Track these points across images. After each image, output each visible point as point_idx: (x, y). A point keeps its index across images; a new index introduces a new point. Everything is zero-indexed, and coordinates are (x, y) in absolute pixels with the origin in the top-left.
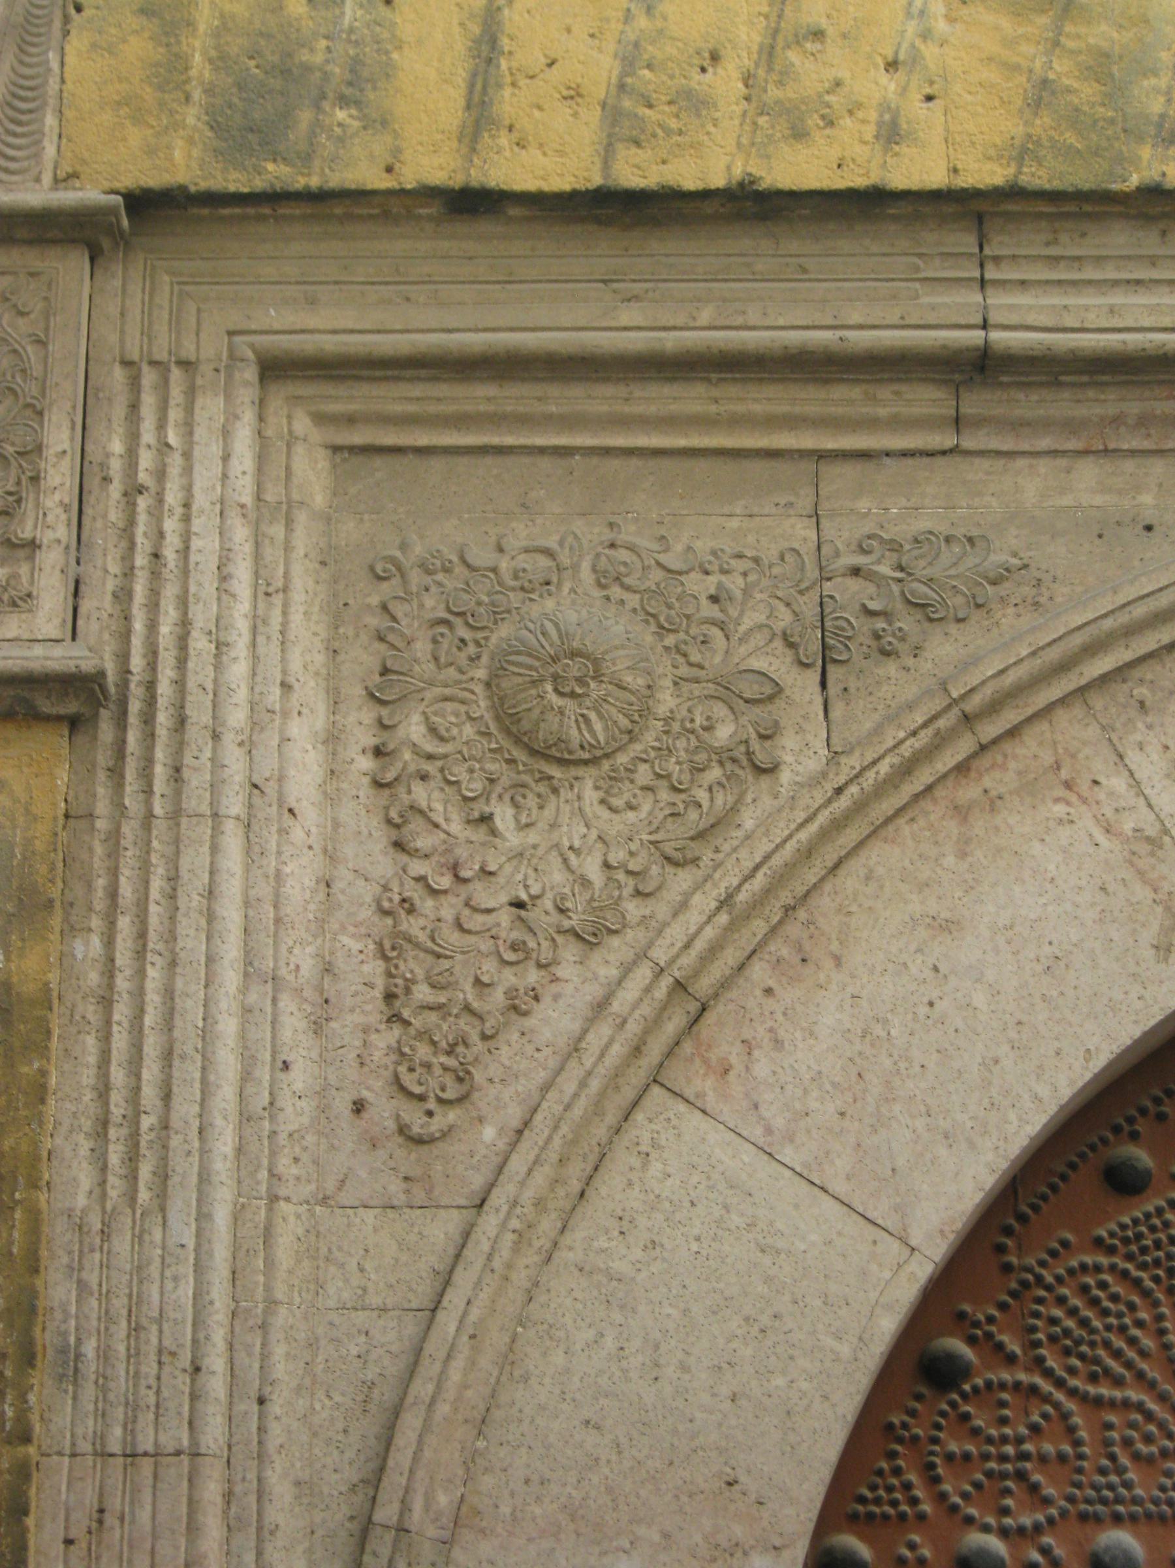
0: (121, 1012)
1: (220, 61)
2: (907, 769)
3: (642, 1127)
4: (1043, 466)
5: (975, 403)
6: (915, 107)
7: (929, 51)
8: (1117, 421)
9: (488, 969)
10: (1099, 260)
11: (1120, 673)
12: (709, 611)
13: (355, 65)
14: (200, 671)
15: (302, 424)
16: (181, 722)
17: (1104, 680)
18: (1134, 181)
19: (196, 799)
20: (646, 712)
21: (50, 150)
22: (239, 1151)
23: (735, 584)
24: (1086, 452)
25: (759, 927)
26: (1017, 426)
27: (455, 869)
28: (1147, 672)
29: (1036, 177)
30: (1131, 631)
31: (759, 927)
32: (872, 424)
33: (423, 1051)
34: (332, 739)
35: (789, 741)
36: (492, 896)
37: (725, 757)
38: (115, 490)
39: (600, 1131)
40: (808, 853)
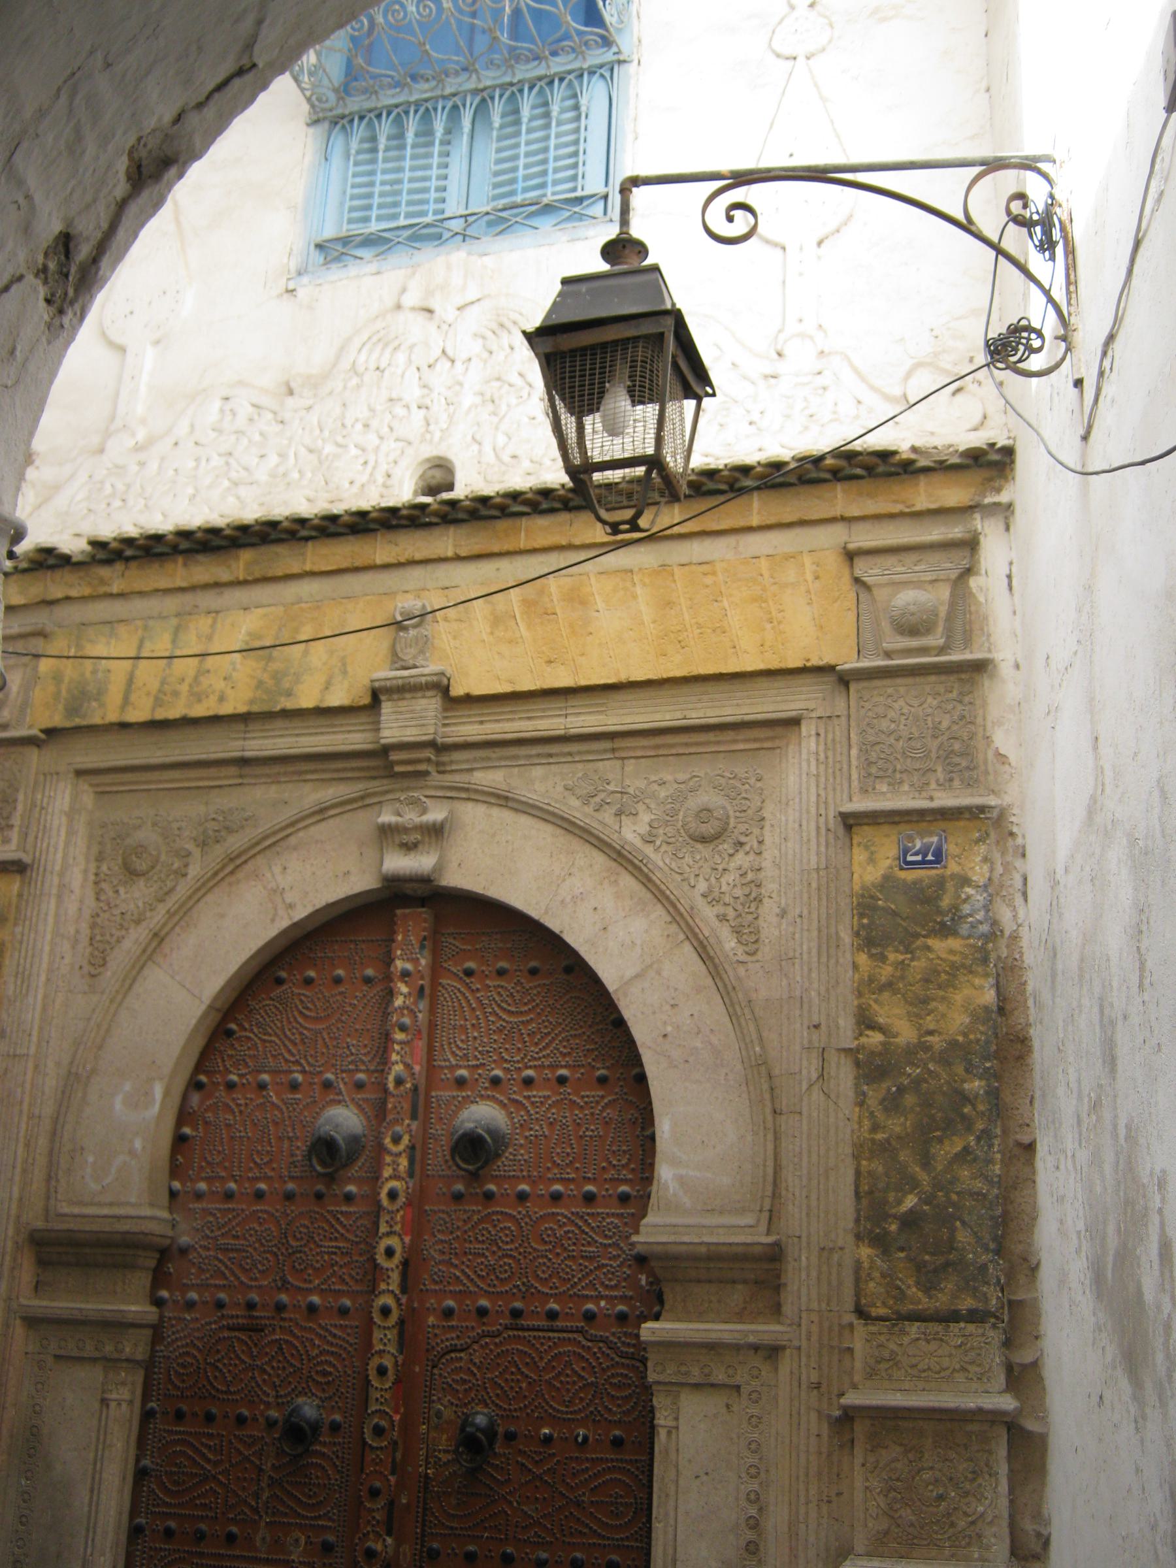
0: (24, 945)
2: (216, 874)
3: (146, 972)
5: (247, 770)
6: (229, 692)
7: (234, 674)
8: (279, 774)
9: (114, 931)
10: (273, 730)
11: (274, 844)
12: (177, 832)
14: (51, 856)
15: (86, 787)
16: (45, 870)
17: (270, 846)
18: (278, 708)
20: (157, 861)
21: (28, 719)
22: (48, 980)
23: (184, 824)
24: (272, 783)
25: (177, 917)
26: (256, 776)
27: (109, 904)
28: (281, 844)
29: (256, 708)
30: (275, 833)
31: (177, 917)
33: (96, 953)
34: (86, 871)
35: (191, 867)
36: (117, 912)
37: (176, 872)
38: (38, 809)
39: (134, 973)
40: (190, 897)
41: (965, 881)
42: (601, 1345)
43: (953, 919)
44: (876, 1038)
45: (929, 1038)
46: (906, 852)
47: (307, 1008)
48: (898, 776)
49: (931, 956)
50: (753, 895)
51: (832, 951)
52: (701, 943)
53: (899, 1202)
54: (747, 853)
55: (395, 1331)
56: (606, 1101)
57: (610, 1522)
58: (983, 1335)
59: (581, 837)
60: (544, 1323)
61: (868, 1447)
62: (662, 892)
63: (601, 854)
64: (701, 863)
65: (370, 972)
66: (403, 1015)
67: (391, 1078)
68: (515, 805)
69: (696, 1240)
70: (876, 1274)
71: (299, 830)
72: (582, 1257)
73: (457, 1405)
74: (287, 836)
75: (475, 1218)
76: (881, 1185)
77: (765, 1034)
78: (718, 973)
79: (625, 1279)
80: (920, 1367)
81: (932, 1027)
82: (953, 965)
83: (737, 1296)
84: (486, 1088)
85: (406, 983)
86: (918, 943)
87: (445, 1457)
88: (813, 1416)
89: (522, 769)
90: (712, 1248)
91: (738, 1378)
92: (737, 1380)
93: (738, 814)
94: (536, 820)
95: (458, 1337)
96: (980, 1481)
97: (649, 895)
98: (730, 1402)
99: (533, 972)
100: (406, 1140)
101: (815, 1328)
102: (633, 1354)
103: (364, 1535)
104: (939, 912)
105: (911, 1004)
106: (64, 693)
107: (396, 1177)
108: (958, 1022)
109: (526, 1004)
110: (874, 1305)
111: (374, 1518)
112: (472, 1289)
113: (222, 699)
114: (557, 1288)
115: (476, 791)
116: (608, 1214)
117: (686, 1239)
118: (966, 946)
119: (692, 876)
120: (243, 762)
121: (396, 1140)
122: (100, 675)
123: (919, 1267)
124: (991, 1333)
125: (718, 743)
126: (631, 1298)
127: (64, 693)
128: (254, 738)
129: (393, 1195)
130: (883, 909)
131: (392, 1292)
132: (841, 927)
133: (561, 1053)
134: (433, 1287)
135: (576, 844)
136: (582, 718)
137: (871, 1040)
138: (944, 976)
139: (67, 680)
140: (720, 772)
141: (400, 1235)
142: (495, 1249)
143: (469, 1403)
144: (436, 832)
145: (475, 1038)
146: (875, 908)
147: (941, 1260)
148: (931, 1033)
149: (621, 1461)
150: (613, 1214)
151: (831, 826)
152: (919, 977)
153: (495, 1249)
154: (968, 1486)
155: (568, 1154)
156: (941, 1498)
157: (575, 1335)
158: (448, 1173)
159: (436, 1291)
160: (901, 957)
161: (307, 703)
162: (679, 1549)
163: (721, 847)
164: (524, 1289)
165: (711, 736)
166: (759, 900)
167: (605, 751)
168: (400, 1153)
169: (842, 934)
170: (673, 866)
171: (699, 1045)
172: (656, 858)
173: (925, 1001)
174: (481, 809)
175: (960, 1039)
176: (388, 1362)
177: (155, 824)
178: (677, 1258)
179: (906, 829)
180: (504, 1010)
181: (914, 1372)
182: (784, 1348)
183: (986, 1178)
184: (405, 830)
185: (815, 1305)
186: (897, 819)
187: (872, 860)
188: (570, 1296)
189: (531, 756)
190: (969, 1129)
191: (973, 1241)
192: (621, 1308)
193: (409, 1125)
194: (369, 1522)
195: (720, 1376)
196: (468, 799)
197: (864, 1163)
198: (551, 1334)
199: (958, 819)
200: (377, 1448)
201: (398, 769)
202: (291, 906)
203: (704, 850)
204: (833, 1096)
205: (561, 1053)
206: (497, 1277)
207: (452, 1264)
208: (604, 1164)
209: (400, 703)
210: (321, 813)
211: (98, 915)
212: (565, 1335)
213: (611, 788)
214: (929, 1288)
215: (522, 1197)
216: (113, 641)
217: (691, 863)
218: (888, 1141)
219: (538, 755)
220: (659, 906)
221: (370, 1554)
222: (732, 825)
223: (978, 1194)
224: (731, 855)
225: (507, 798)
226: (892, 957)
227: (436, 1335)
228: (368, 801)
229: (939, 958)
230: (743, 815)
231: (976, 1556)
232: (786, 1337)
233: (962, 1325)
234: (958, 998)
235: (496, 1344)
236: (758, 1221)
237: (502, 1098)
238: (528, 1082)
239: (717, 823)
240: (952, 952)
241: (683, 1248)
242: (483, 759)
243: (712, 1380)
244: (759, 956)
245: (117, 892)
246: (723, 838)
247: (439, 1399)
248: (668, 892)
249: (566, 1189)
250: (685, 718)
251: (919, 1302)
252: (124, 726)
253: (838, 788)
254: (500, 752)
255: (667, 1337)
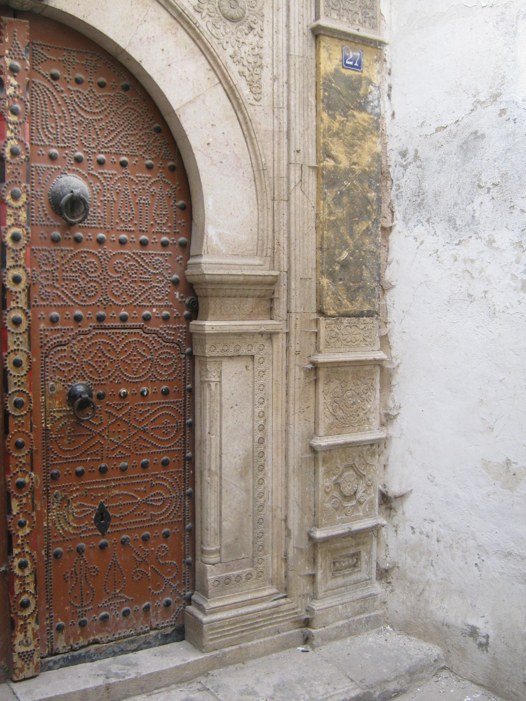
41: (370, 82)
42: (154, 335)
43: (364, 102)
44: (330, 163)
45: (354, 167)
48: (342, 11)
49: (356, 121)
50: (258, 64)
51: (305, 108)
52: (231, 88)
53: (340, 255)
55: (26, 336)
56: (152, 181)
57: (165, 439)
58: (372, 323)
60: (119, 324)
61: (325, 382)
62: (208, 49)
63: (165, 11)
64: (230, 35)
66: (14, 102)
67: (7, 150)
69: (240, 273)
70: (330, 293)
72: (141, 281)
73: (64, 381)
75: (69, 255)
76: (332, 245)
78: (240, 109)
79: (167, 295)
80: (348, 340)
81: (355, 160)
82: (364, 128)
83: (249, 303)
84: (72, 164)
85: (15, 76)
86: (350, 112)
87: (58, 415)
88: (297, 368)
90: (247, 278)
91: (253, 351)
92: (253, 352)
95: (62, 336)
96: (369, 393)
97: (196, 48)
98: (248, 365)
100: (24, 198)
101: (298, 322)
102: (173, 340)
103: (14, 474)
104: (358, 96)
105: (346, 146)
107: (17, 225)
108: (367, 160)
109: (97, 107)
110: (329, 309)
111: (21, 462)
112: (69, 303)
114: (126, 301)
116: (155, 254)
117: (234, 272)
118: (370, 118)
119: (225, 43)
121: (15, 197)
123: (348, 289)
124: (376, 322)
126: (171, 306)
129: (16, 238)
130: (335, 89)
131: (21, 308)
132: (310, 94)
133: (122, 145)
134: (42, 303)
137: (329, 164)
138: (360, 134)
141: (24, 267)
142: (84, 276)
143: (72, 378)
145: (62, 127)
146: (331, 88)
147: (357, 285)
148: (355, 164)
149: (168, 403)
150: (158, 254)
151: (306, 32)
152: (350, 131)
153: (84, 276)
154: (364, 396)
155: (129, 214)
156: (354, 403)
157: (138, 331)
158: (48, 223)
159: (44, 306)
160: (342, 119)
162: (223, 448)
163: (240, 27)
164: (105, 303)
166: (261, 66)
168: (20, 208)
169: (310, 99)
170: (213, 32)
171: (228, 153)
172: (202, 24)
173: (352, 146)
175: (367, 169)
176: (21, 357)
178: (221, 283)
179: (347, 45)
180: (80, 107)
181: (344, 343)
182: (278, 333)
183: (375, 243)
185: (298, 310)
186: (343, 37)
187: (329, 58)
188: (135, 306)
190: (369, 218)
191: (370, 276)
192: (165, 312)
193: (25, 187)
194: (17, 465)
195: (244, 351)
197: (325, 232)
198: (123, 331)
199: (368, 46)
200: (19, 416)
203: (231, 27)
204: (306, 193)
205: (122, 145)
206: (87, 295)
207: (55, 287)
208: (152, 222)
212: (132, 331)
214: (352, 300)
215: (100, 242)
217: (224, 33)
218: (335, 220)
220: (203, 57)
221: (20, 486)
222: (247, 14)
223: (372, 252)
224: (246, 34)
226: (339, 117)
227: (46, 336)
229: (359, 123)
230: (252, 9)
231: (367, 428)
232: (280, 327)
233: (365, 318)
234: (367, 146)
235: (88, 339)
236: (265, 262)
237: (84, 173)
238: (101, 163)
239: (241, 11)
240: (364, 120)
241: (231, 278)
243: (241, 353)
244: (262, 103)
246: (242, 22)
247: (51, 378)
248: (212, 50)
249: (129, 237)
251: (348, 307)
253: (309, 8)
255: (220, 330)
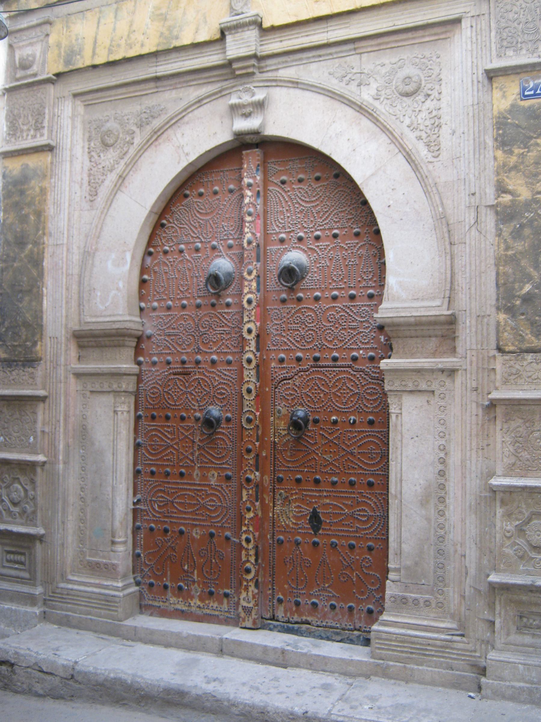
0: (56, 188)
1: (65, 52)
2: (148, 141)
3: (117, 196)
4: (169, 92)
5: (159, 84)
8: (176, 83)
9: (100, 177)
10: (171, 59)
11: (176, 122)
13: (80, 49)
14: (65, 141)
18: (172, 46)
19: (64, 159)
20: (118, 138)
22: (70, 205)
23: (130, 117)
24: (174, 89)
25: (130, 166)
26: (164, 86)
27: (96, 163)
28: (180, 121)
29: (160, 48)
30: (176, 116)
31: (130, 166)
32: (146, 90)
33: (92, 189)
34: (83, 147)
37: (128, 142)
39: (112, 197)
40: (136, 155)
44: (507, 198)
46: (524, 89)
47: (201, 209)
50: (436, 124)
52: (407, 153)
53: (521, 289)
54: (432, 100)
55: (254, 371)
59: (339, 101)
61: (504, 420)
62: (385, 127)
63: (350, 109)
64: (406, 108)
65: (232, 187)
66: (249, 207)
67: (245, 241)
68: (302, 86)
69: (409, 315)
70: (508, 328)
71: (189, 113)
74: (184, 117)
75: (293, 311)
76: (511, 280)
77: (445, 201)
78: (417, 169)
79: (373, 339)
80: (533, 377)
83: (433, 343)
84: (295, 243)
86: (532, 142)
87: (284, 433)
88: (474, 405)
89: (305, 66)
90: (418, 318)
92: (433, 388)
93: (426, 78)
94: (314, 93)
97: (378, 129)
98: (429, 399)
99: (318, 179)
100: (254, 273)
101: (474, 359)
105: (528, 177)
106: (63, 53)
107: (250, 292)
109: (314, 197)
110: (507, 345)
113: (142, 45)
115: (281, 81)
117: (403, 314)
119: (402, 116)
120: (157, 79)
121: (250, 273)
122: (80, 41)
125: (414, 38)
126: (376, 348)
127: (63, 53)
128: (161, 65)
129: (249, 302)
130: (511, 124)
132: (487, 137)
135: (336, 105)
136: (336, 32)
137: (505, 199)
139: (63, 46)
140: (415, 55)
144: (260, 105)
145: (288, 217)
146: (506, 124)
149: (373, 432)
150: (365, 305)
151: (480, 79)
152: (532, 161)
157: (347, 369)
158: (278, 289)
160: (522, 151)
161: (186, 41)
162: (403, 475)
163: (417, 98)
165: (410, 35)
166: (439, 126)
167: (350, 50)
169: (487, 141)
170: (391, 111)
174: (284, 90)
176: (252, 387)
177: (115, 119)
178: (398, 325)
179: (525, 76)
180: (303, 200)
181: (530, 380)
182: (457, 370)
184: (244, 106)
185: (474, 347)
186: (519, 71)
187: (504, 96)
189: (308, 58)
192: (371, 354)
195: (423, 386)
196: (277, 86)
197: (501, 268)
198: (335, 369)
201: (238, 73)
202: (187, 154)
204: (483, 232)
209: (236, 35)
210: (199, 102)
211: (91, 169)
213: (354, 71)
215: (317, 299)
216: (85, 22)
217: (401, 109)
218: (514, 255)
219: (314, 57)
220: (384, 135)
221: (248, 480)
222: (423, 85)
224: (423, 102)
225: (297, 83)
226: (516, 151)
228: (224, 93)
232: (459, 364)
236: (443, 303)
238: (317, 238)
241: (402, 320)
242: (283, 62)
243: (419, 388)
244: (440, 158)
245: (100, 156)
248: (388, 126)
249: (340, 293)
250: (394, 25)
252: (94, 67)
253: (484, 56)
254: (292, 57)
